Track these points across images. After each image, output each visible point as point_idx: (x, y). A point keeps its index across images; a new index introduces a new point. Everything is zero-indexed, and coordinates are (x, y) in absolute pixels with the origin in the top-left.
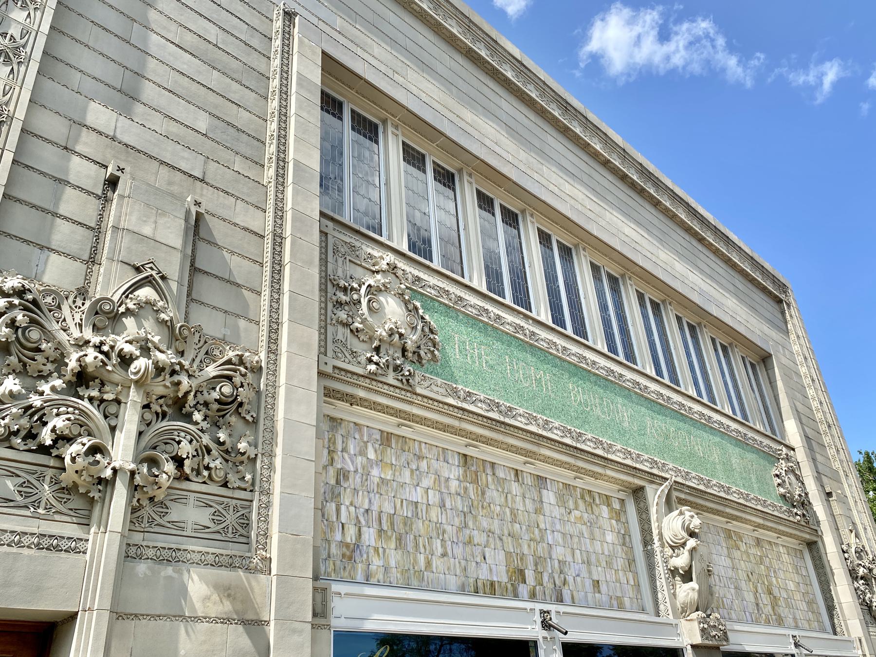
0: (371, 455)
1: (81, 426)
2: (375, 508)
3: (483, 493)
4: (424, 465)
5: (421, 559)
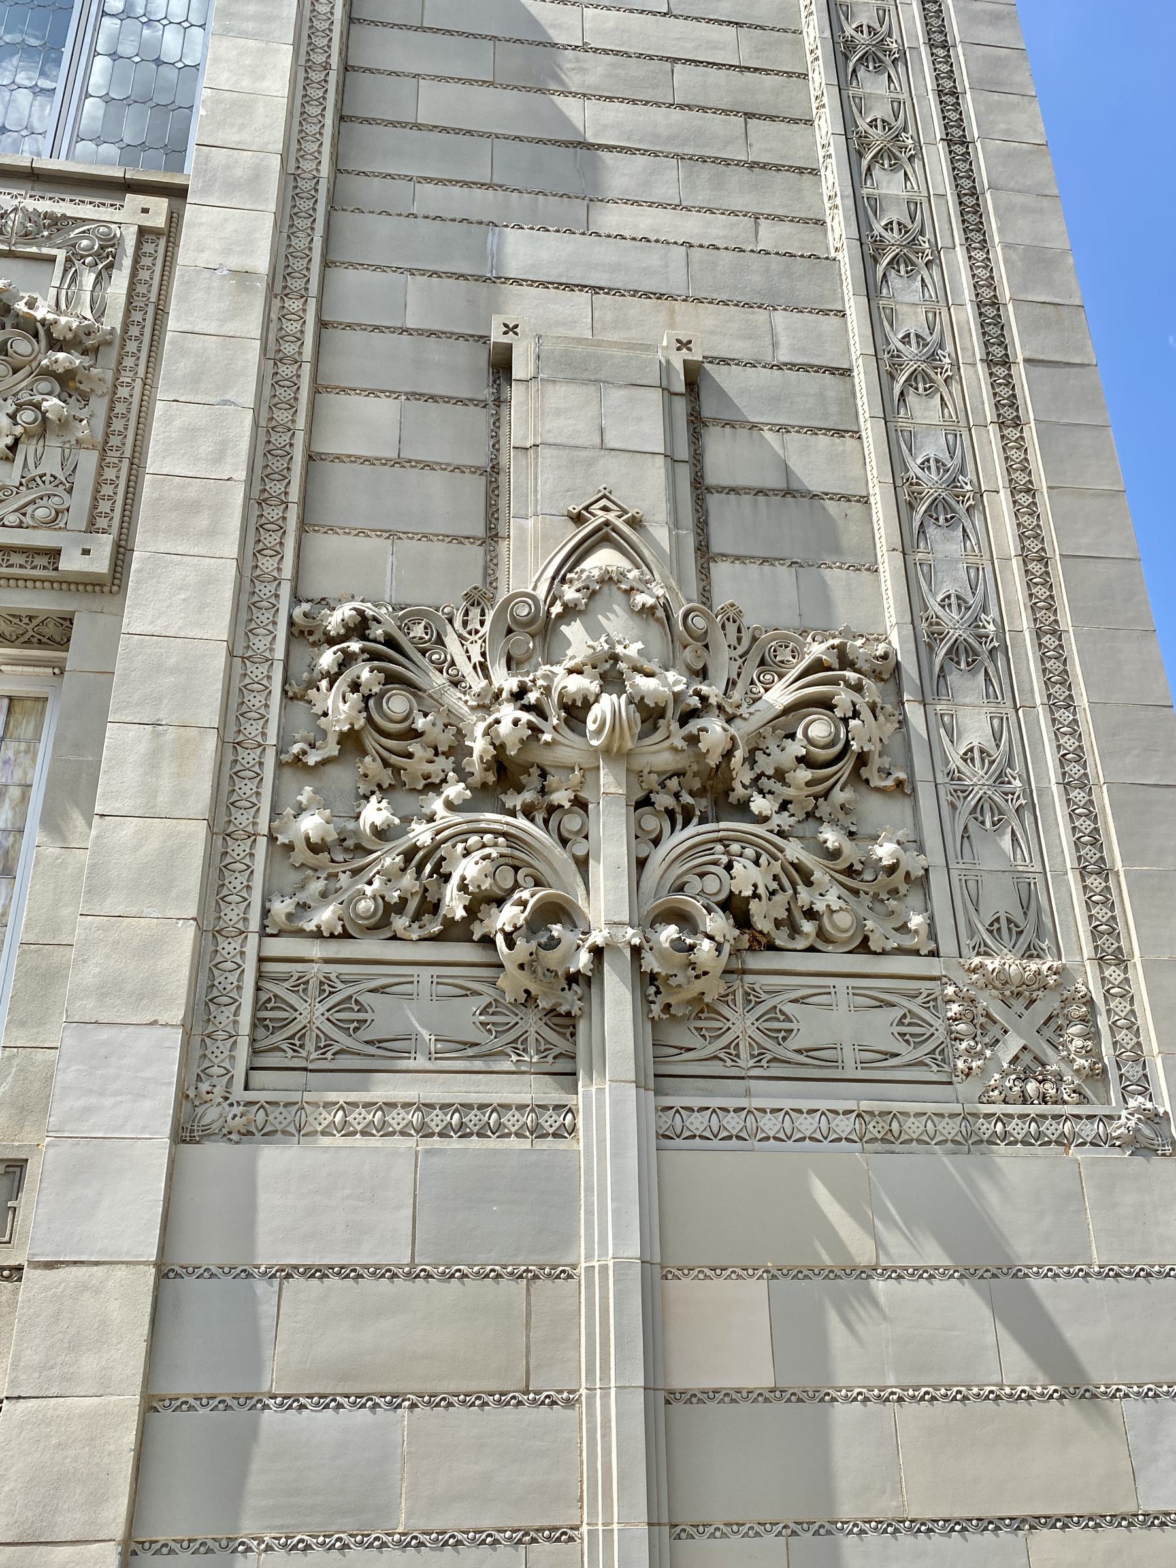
1: (516, 869)
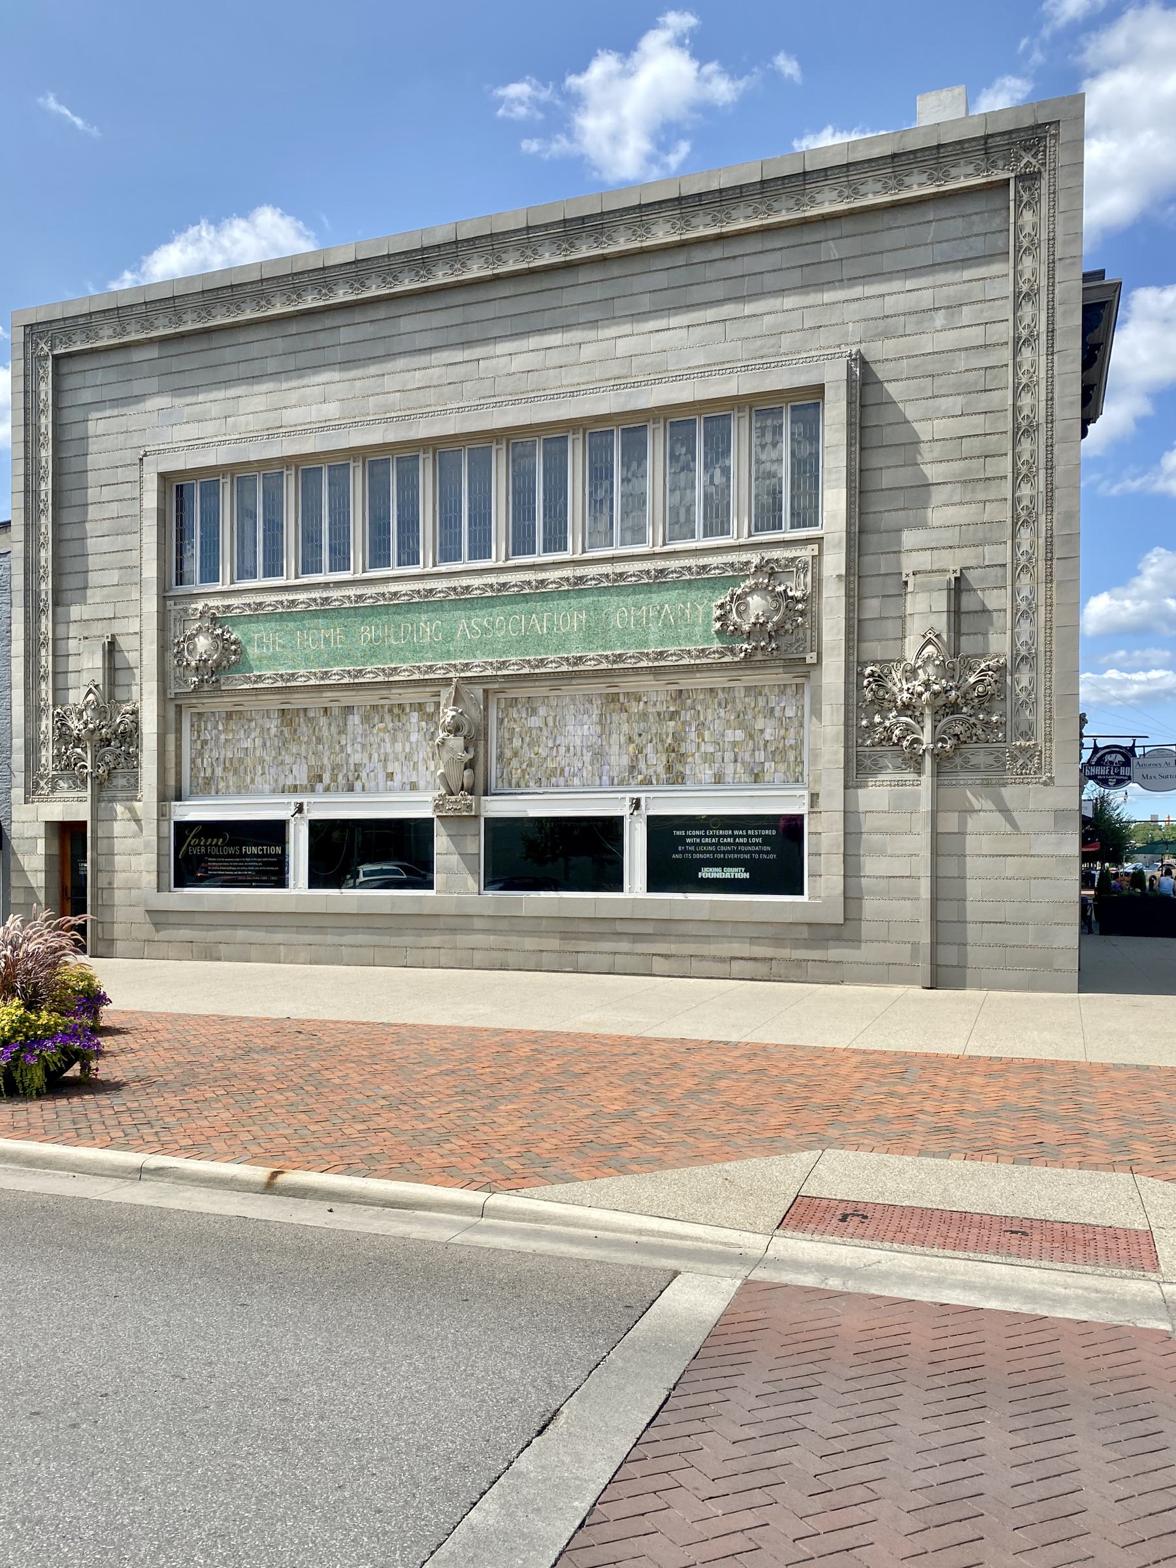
0: (221, 728)
2: (222, 757)
3: (295, 731)
4: (253, 724)
5: (248, 779)
